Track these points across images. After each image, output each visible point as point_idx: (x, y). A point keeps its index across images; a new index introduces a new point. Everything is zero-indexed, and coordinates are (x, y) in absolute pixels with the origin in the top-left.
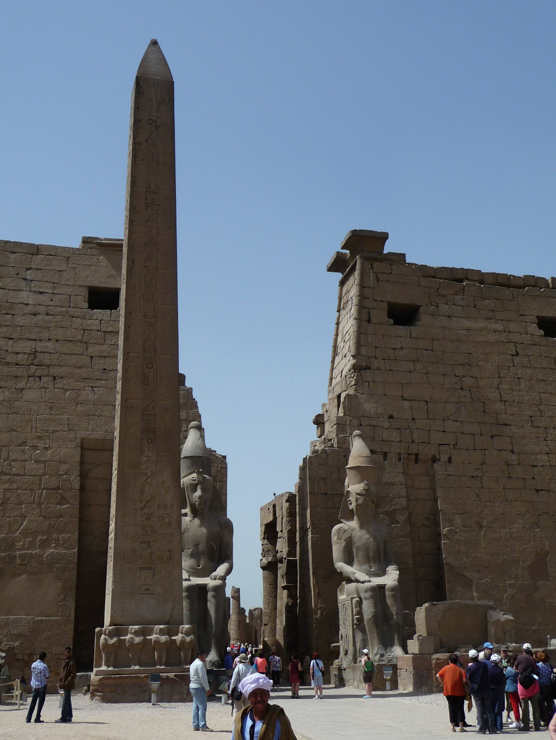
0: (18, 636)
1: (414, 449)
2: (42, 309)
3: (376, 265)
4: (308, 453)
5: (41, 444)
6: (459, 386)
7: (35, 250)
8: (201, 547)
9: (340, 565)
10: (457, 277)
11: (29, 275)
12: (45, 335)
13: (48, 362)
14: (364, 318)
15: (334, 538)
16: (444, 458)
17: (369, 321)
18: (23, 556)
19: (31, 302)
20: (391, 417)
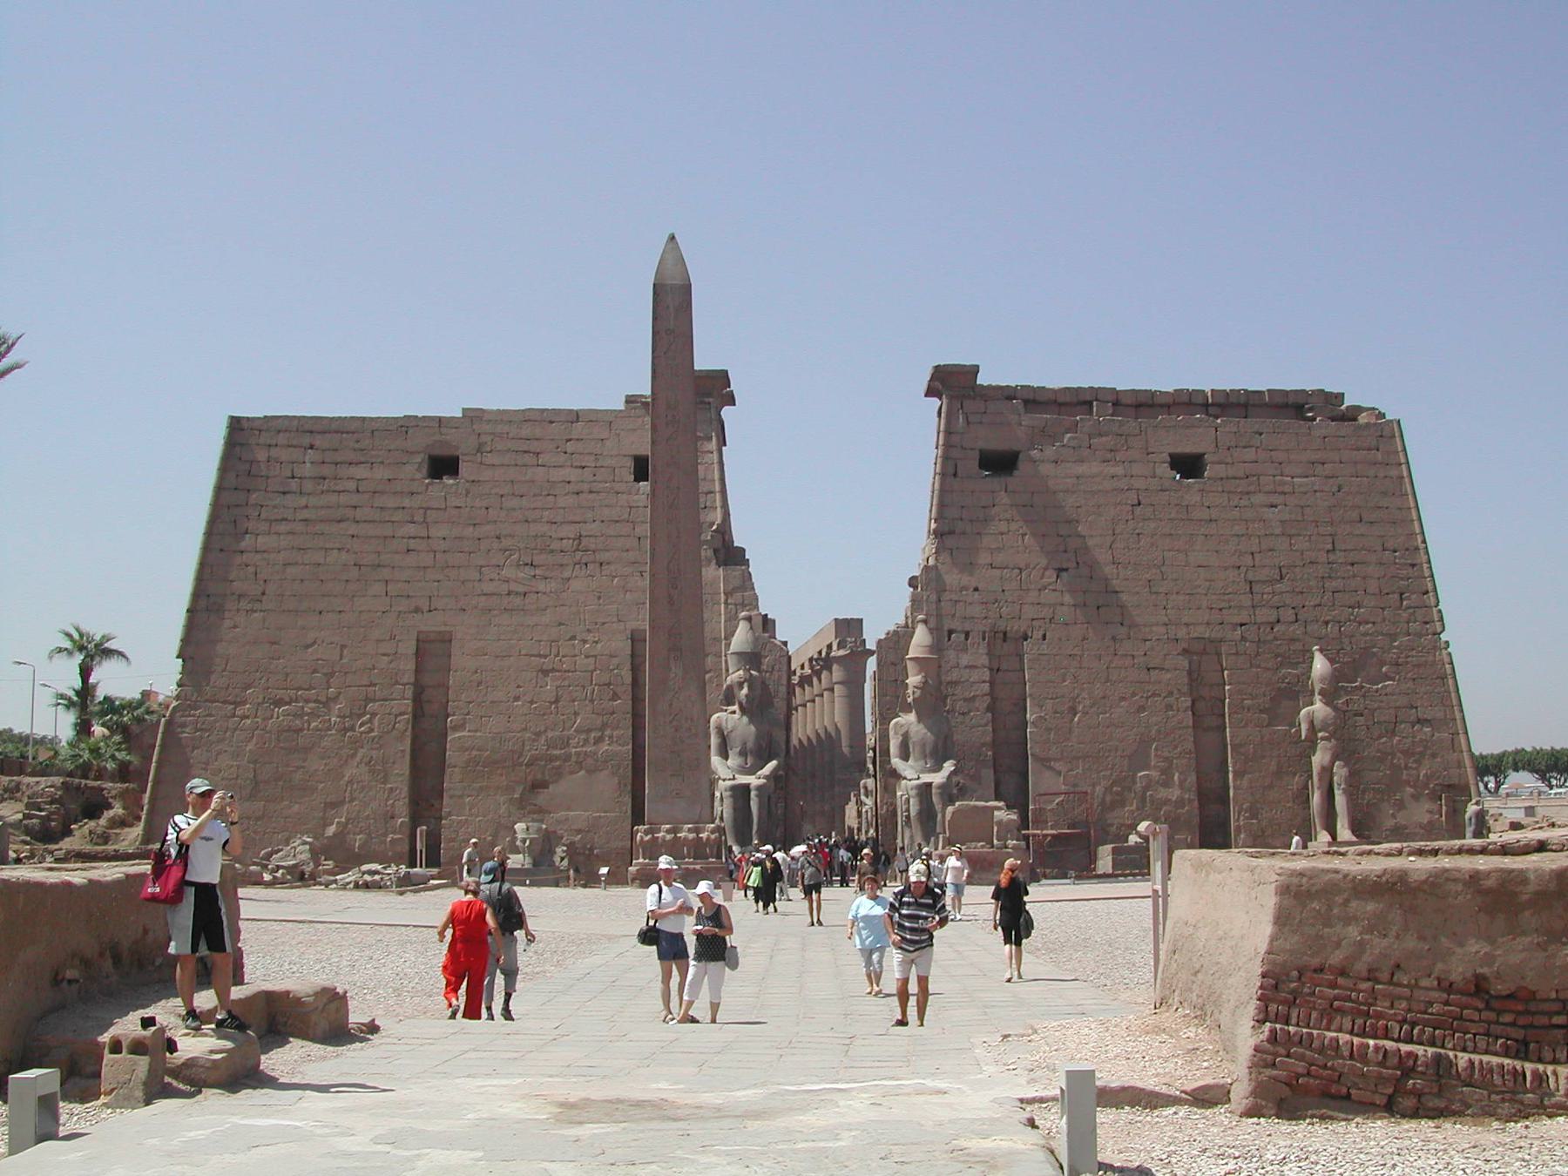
0: (579, 831)
1: (1002, 625)
2: (586, 487)
3: (967, 403)
4: (892, 628)
5: (590, 637)
6: (1062, 548)
7: (575, 416)
8: (750, 745)
9: (896, 762)
10: (1079, 402)
11: (570, 447)
12: (589, 515)
13: (593, 547)
14: (949, 471)
15: (891, 733)
16: (1038, 634)
17: (955, 475)
18: (578, 754)
19: (572, 479)
20: (976, 589)
